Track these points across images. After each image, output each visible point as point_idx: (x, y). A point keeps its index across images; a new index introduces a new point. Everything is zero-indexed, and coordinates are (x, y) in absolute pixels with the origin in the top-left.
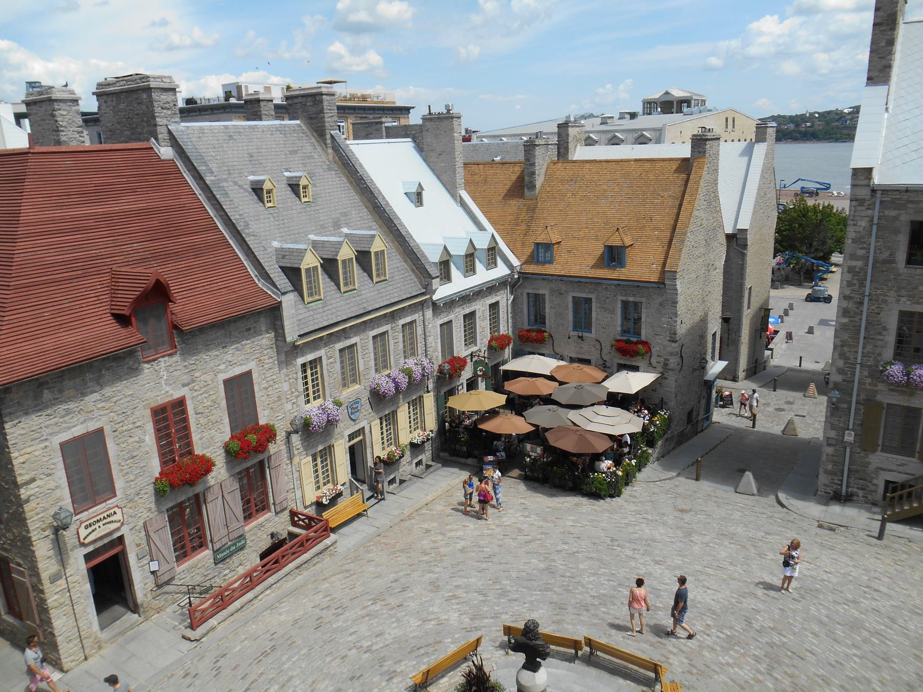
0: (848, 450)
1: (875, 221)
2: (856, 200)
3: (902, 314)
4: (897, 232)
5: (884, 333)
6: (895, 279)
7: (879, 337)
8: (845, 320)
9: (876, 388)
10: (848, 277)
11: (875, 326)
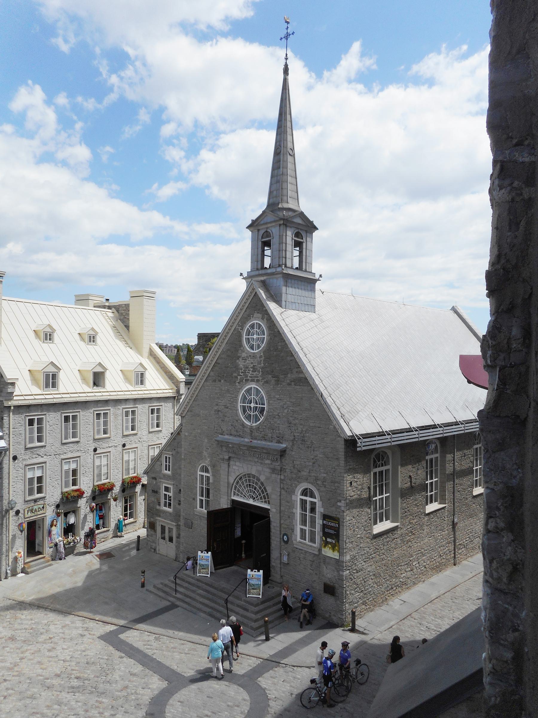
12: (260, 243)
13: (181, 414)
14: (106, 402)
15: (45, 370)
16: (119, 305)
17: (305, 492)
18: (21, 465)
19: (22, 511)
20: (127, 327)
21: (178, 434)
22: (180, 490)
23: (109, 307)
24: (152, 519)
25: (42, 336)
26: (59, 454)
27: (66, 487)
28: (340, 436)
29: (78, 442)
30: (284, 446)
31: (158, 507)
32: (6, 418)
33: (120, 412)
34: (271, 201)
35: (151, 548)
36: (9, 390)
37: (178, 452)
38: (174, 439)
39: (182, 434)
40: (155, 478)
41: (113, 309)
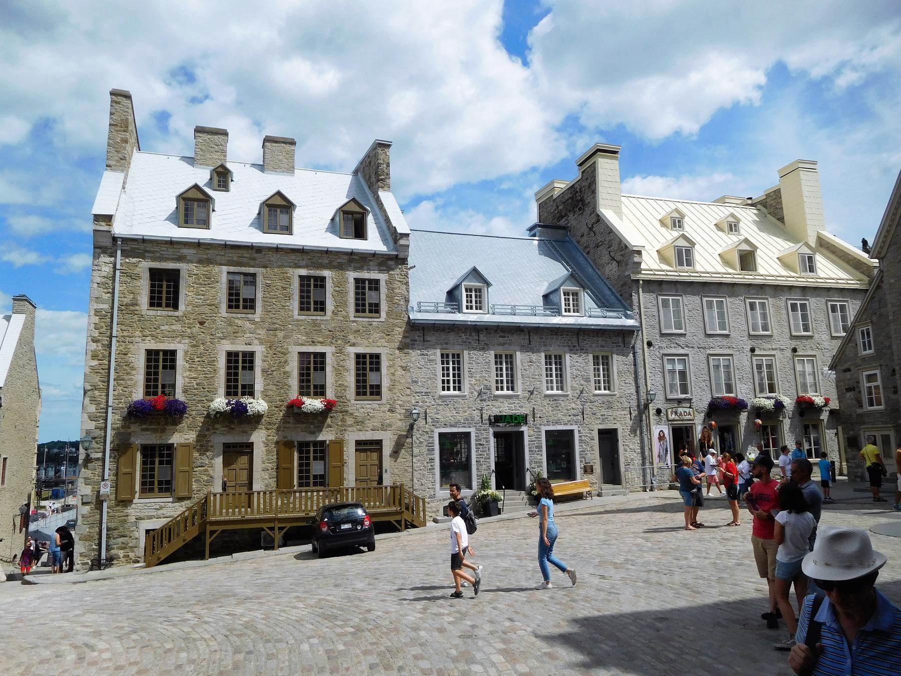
0: (105, 505)
1: (118, 267)
2: (100, 248)
3: (149, 352)
4: (135, 277)
5: (134, 372)
6: (139, 321)
7: (126, 377)
8: (95, 362)
9: (129, 431)
10: (96, 319)
11: (125, 367)
13: (879, 253)
14: (762, 287)
15: (675, 244)
16: (768, 195)
18: (657, 354)
19: (663, 411)
20: (781, 219)
21: (879, 287)
22: (894, 370)
23: (752, 205)
24: (851, 433)
25: (669, 222)
26: (704, 348)
27: (717, 392)
29: (727, 336)
31: (859, 411)
32: (635, 297)
33: (783, 304)
35: (856, 477)
36: (636, 259)
37: (881, 315)
38: (873, 298)
39: (885, 286)
40: (849, 370)
41: (759, 206)
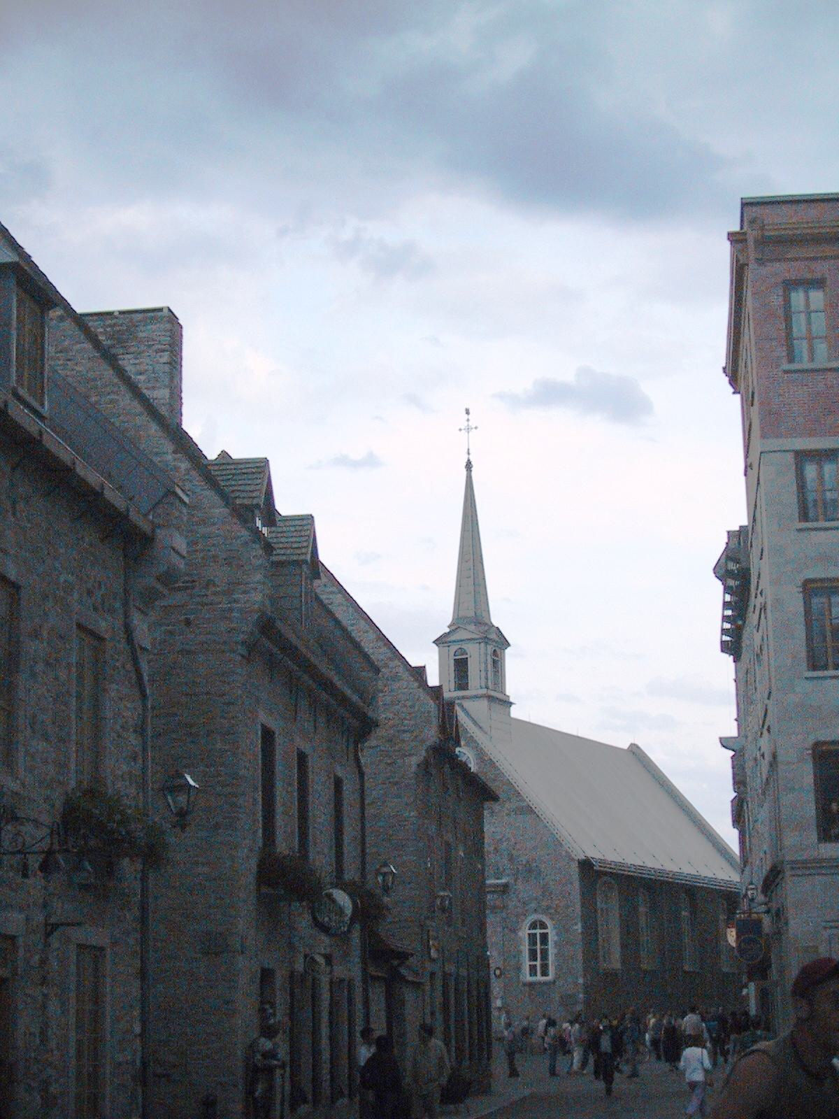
12: (452, 662)
17: (533, 926)
28: (573, 859)
30: (503, 881)
34: (462, 614)
